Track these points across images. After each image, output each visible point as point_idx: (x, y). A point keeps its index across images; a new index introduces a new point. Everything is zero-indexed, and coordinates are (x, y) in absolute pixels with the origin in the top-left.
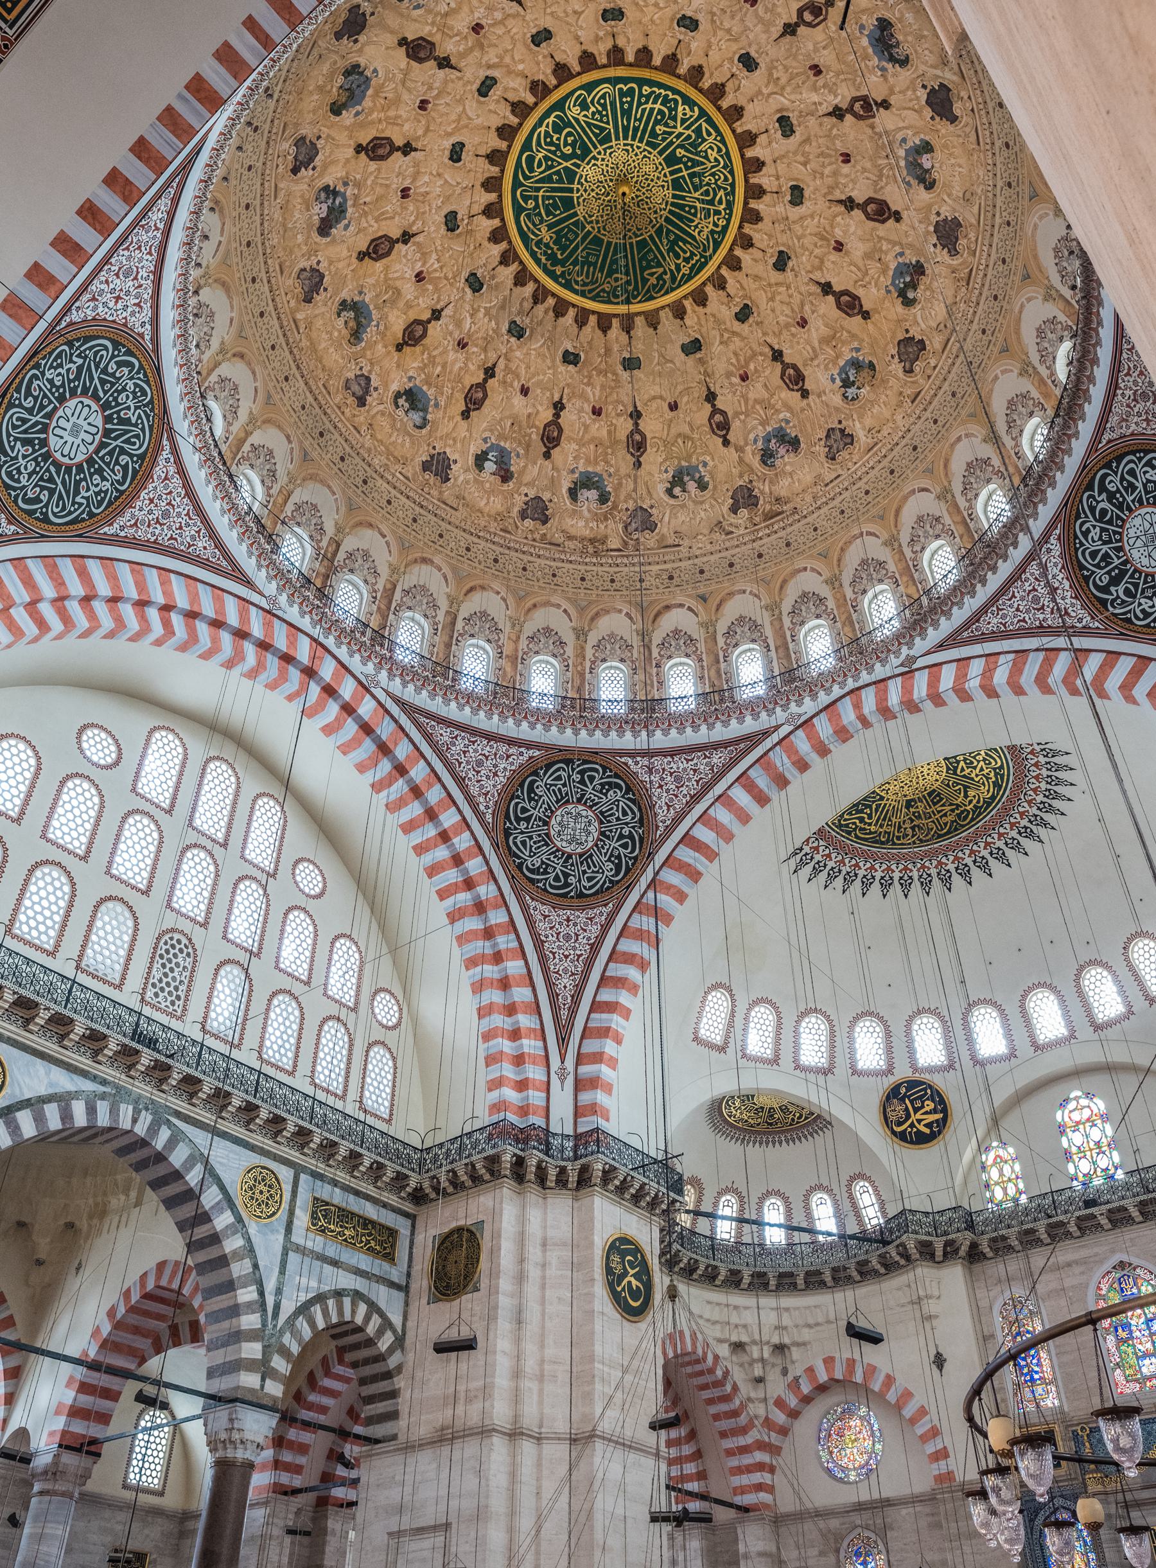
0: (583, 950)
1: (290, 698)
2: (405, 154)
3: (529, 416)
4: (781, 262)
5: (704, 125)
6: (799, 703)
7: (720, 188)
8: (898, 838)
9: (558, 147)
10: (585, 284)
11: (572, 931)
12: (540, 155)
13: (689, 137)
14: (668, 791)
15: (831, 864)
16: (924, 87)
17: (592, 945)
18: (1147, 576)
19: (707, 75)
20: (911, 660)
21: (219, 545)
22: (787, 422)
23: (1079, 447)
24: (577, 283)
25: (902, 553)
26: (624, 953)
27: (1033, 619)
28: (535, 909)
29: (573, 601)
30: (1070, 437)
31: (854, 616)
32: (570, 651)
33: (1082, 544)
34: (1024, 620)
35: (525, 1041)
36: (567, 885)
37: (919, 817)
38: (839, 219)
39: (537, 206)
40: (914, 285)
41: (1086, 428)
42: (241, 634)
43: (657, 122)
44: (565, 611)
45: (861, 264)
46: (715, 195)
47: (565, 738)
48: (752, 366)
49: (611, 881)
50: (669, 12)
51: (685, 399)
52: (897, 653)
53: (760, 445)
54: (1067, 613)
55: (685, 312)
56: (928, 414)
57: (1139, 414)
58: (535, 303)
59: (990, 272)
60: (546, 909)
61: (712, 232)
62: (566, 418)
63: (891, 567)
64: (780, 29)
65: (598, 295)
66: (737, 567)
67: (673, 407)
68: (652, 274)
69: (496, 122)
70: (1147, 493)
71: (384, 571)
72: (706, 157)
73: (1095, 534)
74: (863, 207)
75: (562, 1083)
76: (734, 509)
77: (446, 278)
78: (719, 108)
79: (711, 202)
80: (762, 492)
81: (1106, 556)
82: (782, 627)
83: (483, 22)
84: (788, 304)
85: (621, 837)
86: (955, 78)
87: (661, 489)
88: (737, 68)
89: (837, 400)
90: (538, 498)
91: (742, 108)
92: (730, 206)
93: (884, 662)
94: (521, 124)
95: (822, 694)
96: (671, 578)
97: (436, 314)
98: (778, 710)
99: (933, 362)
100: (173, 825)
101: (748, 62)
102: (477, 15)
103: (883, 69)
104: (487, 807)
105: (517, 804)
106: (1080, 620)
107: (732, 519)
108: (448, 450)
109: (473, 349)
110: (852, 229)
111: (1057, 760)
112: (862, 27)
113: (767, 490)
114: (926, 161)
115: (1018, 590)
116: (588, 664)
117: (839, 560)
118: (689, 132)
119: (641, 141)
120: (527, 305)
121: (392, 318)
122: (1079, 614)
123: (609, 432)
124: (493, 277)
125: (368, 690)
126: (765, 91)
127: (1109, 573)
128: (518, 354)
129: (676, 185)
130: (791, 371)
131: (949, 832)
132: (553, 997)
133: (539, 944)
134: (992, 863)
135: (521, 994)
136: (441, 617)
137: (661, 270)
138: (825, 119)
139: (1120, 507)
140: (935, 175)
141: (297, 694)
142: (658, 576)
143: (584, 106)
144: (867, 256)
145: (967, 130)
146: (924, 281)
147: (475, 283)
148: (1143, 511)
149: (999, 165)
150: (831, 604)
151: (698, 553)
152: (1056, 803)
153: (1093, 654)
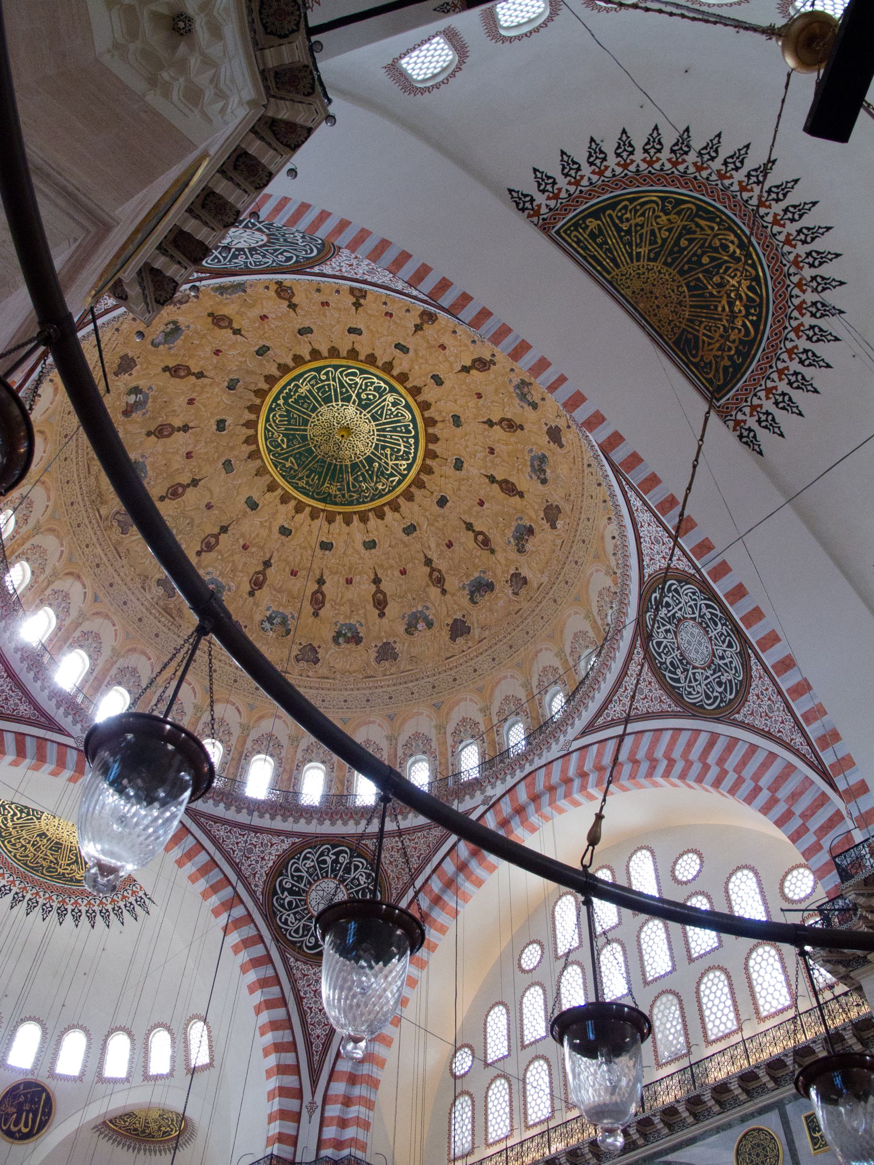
2: (354, 304)
3: (174, 411)
4: (326, 546)
5: (397, 479)
7: (360, 494)
8: (9, 842)
9: (365, 390)
10: (274, 421)
12: (358, 380)
13: (387, 470)
16: (464, 616)
18: (306, 909)
19: (429, 477)
22: (229, 590)
24: (274, 415)
27: (238, 856)
30: (351, 817)
33: (298, 859)
37: (33, 845)
38: (366, 577)
39: (323, 381)
40: (348, 641)
43: (392, 449)
44: (47, 506)
45: (344, 600)
46: (354, 492)
48: (254, 550)
50: (464, 453)
51: (217, 512)
54: (254, 875)
55: (273, 491)
57: (392, 856)
58: (255, 391)
59: (380, 690)
61: (330, 495)
62: (180, 436)
64: (468, 521)
65: (269, 431)
66: (125, 608)
67: (209, 507)
68: (292, 463)
69: (378, 353)
72: (377, 482)
73: (309, 863)
74: (379, 591)
77: (265, 333)
78: (410, 486)
79: (349, 490)
81: (300, 878)
82: (108, 670)
83: (447, 351)
84: (302, 559)
86: (477, 637)
88: (437, 496)
89: (258, 617)
91: (413, 500)
92: (351, 503)
94: (378, 367)
96: (98, 566)
97: (237, 332)
99: (310, 674)
101: (442, 502)
102: (452, 349)
103: (464, 588)
107: (153, 584)
108: (138, 367)
109: (215, 359)
110: (362, 587)
111: (137, 908)
112: (484, 572)
114: (421, 626)
116: (20, 551)
118: (390, 470)
119: (378, 440)
120: (253, 387)
121: (232, 306)
122: (259, 883)
123: (178, 470)
124: (268, 361)
126: (427, 514)
127: (293, 885)
128: (217, 390)
129: (354, 466)
130: (261, 578)
131: (32, 868)
137: (296, 468)
138: (422, 555)
139: (333, 870)
140: (416, 634)
143: (394, 404)
144: (350, 601)
145: (450, 649)
146: (352, 646)
147: (262, 351)
149: (441, 676)
151: (122, 574)
153: (242, 906)
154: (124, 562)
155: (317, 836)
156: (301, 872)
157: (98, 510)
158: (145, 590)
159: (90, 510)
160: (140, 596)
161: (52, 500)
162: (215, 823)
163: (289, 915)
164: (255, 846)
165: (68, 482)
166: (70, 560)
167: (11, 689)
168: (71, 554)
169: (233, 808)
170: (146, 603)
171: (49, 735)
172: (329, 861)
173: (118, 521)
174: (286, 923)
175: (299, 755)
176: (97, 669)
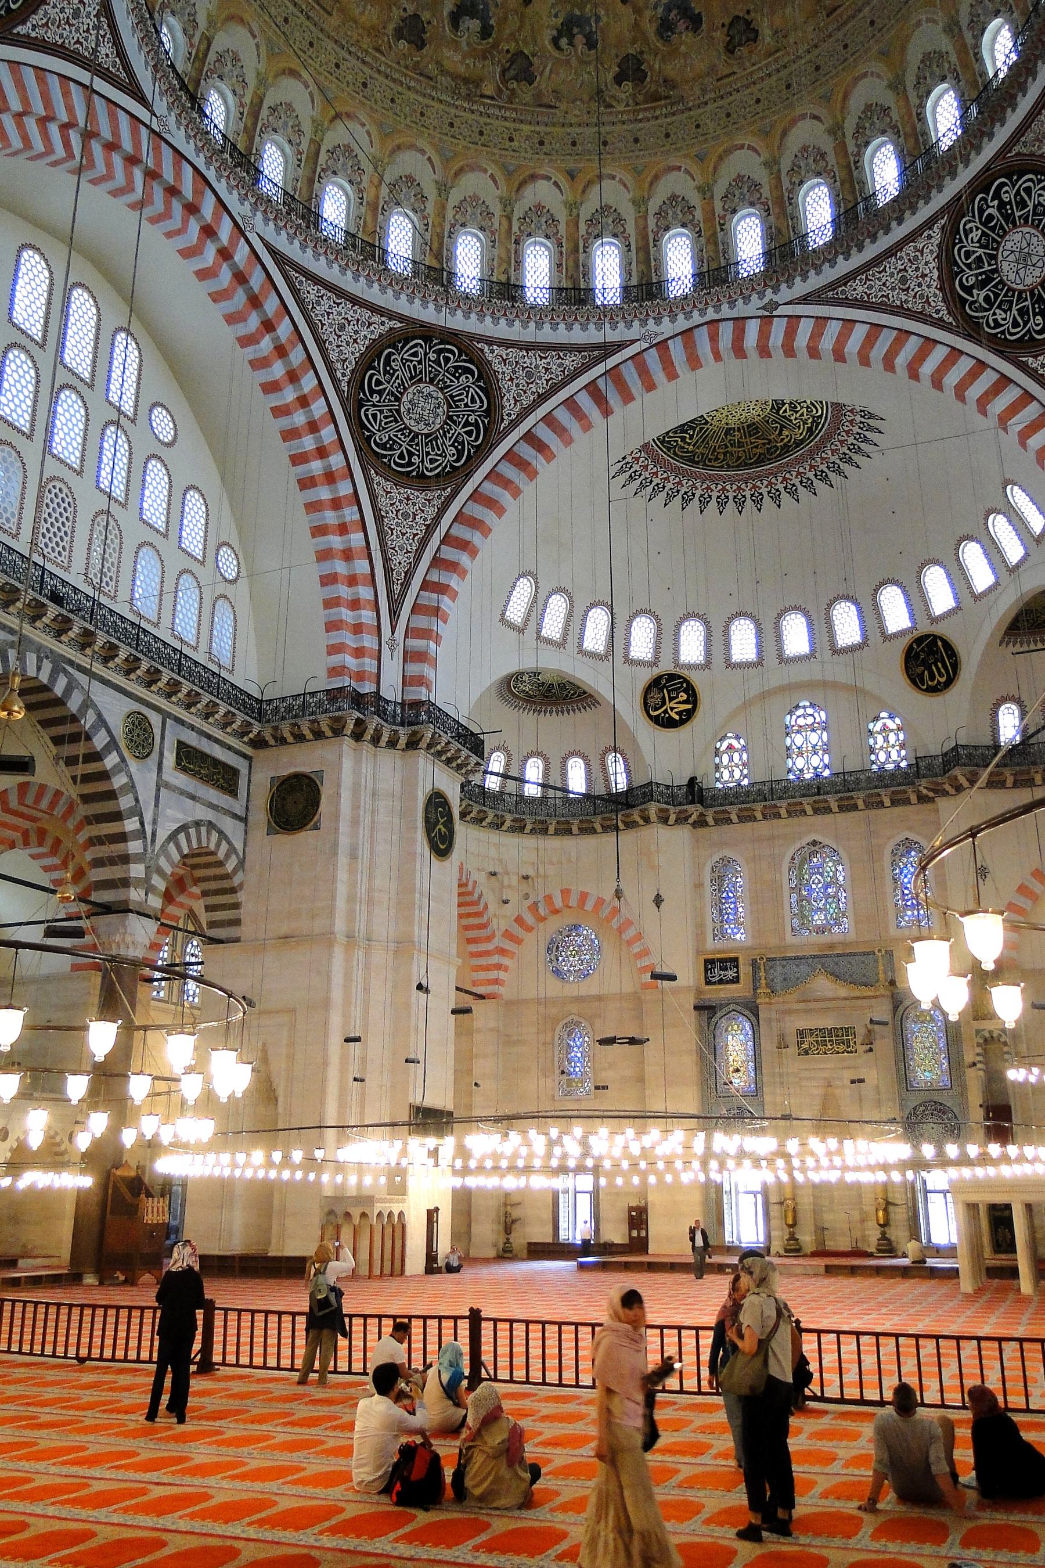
0: (420, 530)
1: (169, 235)
6: (658, 321)
8: (710, 460)
11: (411, 509)
14: (517, 385)
15: (656, 481)
17: (428, 526)
20: (774, 305)
21: (121, 54)
23: (990, 149)
25: (779, 178)
26: (457, 539)
27: (896, 297)
28: (378, 484)
29: (440, 151)
30: (983, 134)
31: (720, 235)
32: (430, 207)
33: (961, 241)
34: (887, 296)
35: (363, 612)
36: (410, 464)
41: (1002, 134)
42: (172, 191)
44: (429, 159)
47: (428, 314)
49: (452, 466)
52: (761, 295)
53: (660, 10)
54: (928, 302)
56: (840, 35)
60: (388, 485)
63: (766, 191)
70: (1035, 214)
71: (307, 127)
73: (975, 235)
75: (392, 651)
76: (619, 80)
80: (651, 68)
81: (979, 258)
82: (646, 227)
85: (467, 424)
87: (547, 35)
90: (416, 16)
93: (747, 300)
95: (681, 317)
98: (636, 323)
100: (46, 359)
104: (344, 375)
105: (372, 375)
106: (938, 312)
107: (614, 90)
111: (871, 422)
113: (657, 66)
115: (893, 265)
116: (447, 228)
117: (715, 168)
122: (939, 306)
125: (242, 233)
127: (976, 275)
132: (388, 572)
133: (379, 519)
134: (784, 495)
135: (362, 566)
136: (304, 146)
139: (1007, 217)
141: (179, 232)
142: (528, 138)
148: (1026, 229)
150: (699, 214)
152: (856, 458)
154: (563, 106)
155: (958, 197)
156: (974, 252)
157: (482, 96)
158: (610, 106)
159: (475, 107)
160: (612, 118)
161: (427, 148)
162: (845, 284)
163: (994, 314)
164: (905, 270)
165: (422, 114)
166: (509, 174)
167: (541, 358)
168: (504, 167)
169: (854, 251)
170: (625, 117)
171: (612, 362)
172: (993, 211)
173: (515, 78)
174: (997, 325)
175: (914, 100)
176: (632, 240)
